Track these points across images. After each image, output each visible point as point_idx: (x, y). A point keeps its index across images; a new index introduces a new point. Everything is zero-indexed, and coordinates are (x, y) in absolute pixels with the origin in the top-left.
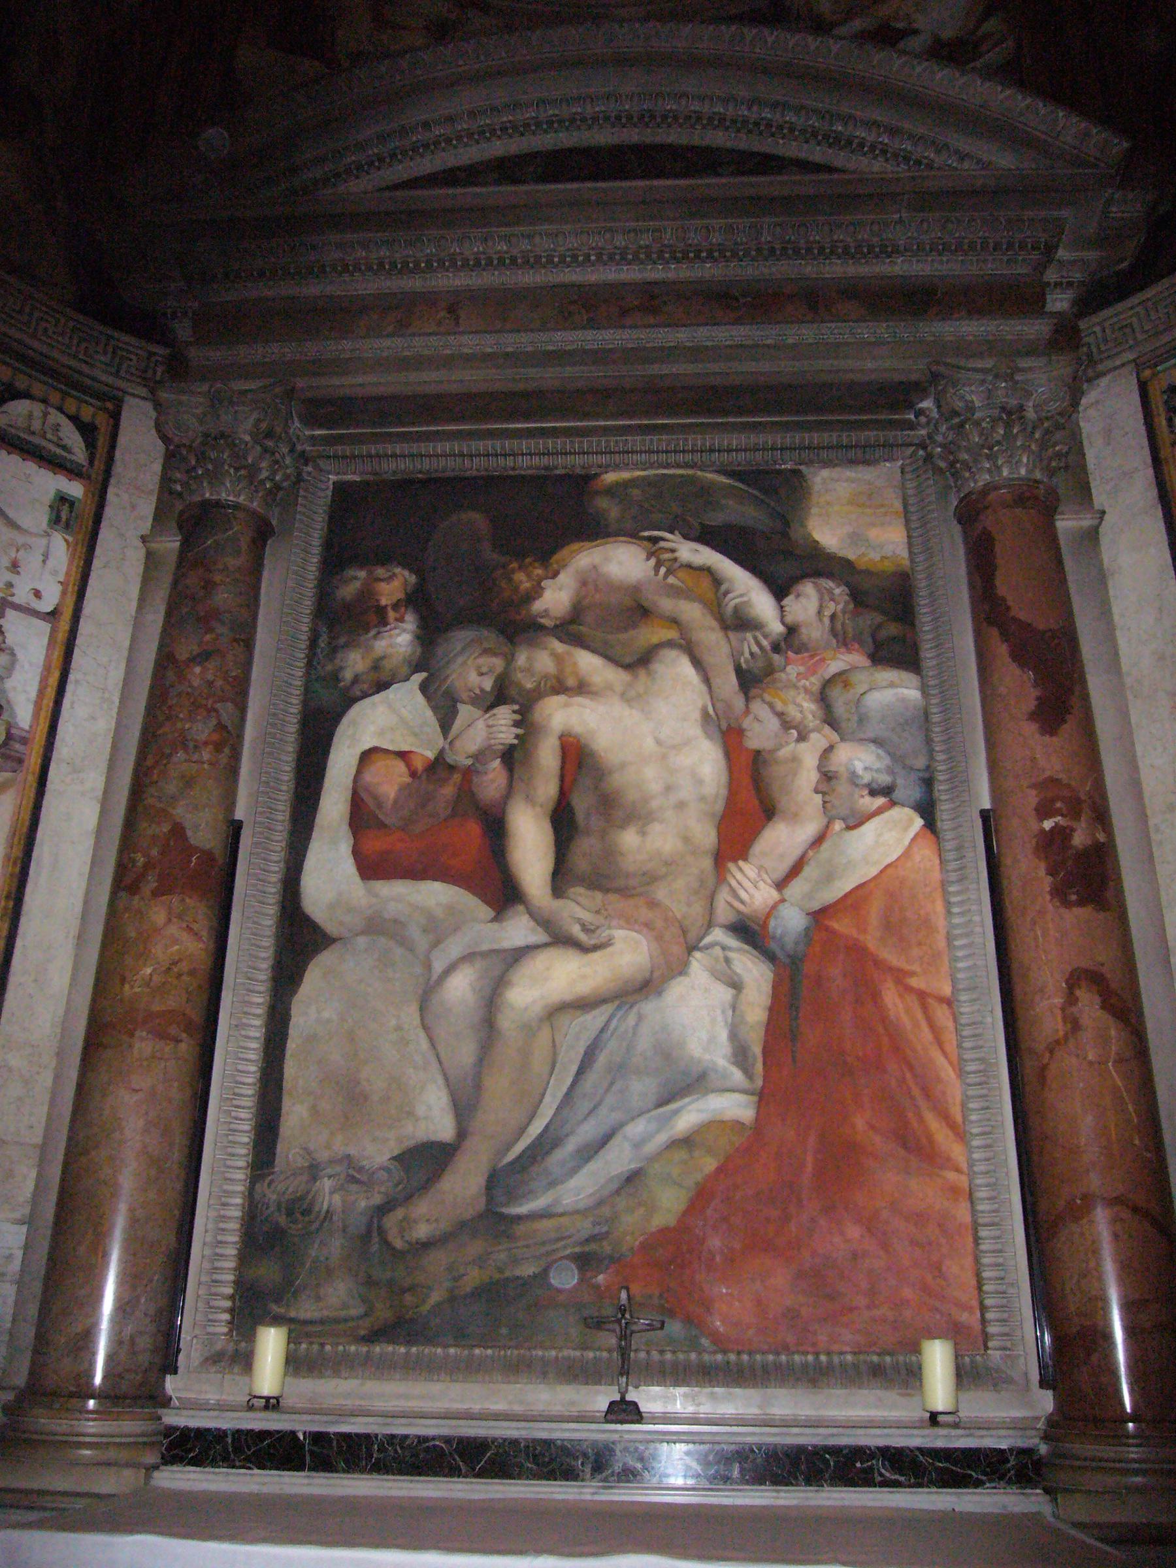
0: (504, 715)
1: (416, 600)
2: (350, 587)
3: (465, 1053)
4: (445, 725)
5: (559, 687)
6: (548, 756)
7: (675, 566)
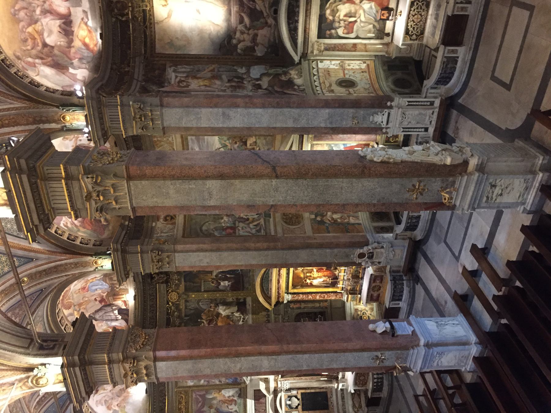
0: (341, 22)
1: (330, 30)
2: (328, 36)
3: (367, 24)
4: (341, 27)
5: (339, 17)
6: (345, 18)
7: (329, 7)
